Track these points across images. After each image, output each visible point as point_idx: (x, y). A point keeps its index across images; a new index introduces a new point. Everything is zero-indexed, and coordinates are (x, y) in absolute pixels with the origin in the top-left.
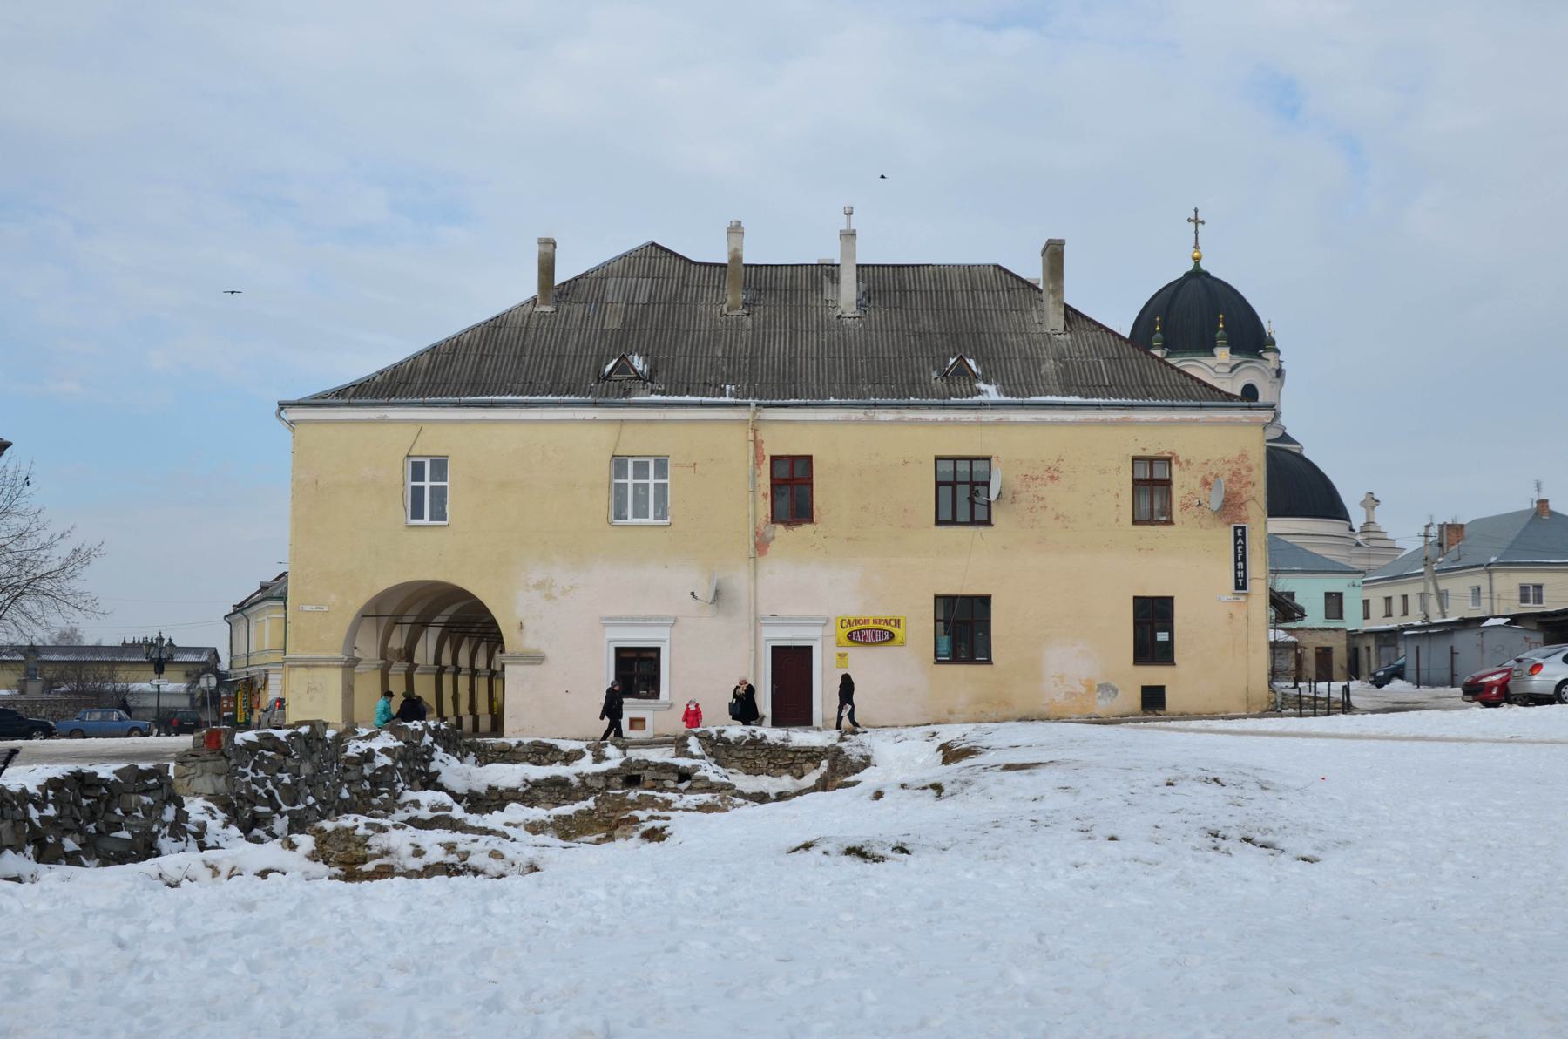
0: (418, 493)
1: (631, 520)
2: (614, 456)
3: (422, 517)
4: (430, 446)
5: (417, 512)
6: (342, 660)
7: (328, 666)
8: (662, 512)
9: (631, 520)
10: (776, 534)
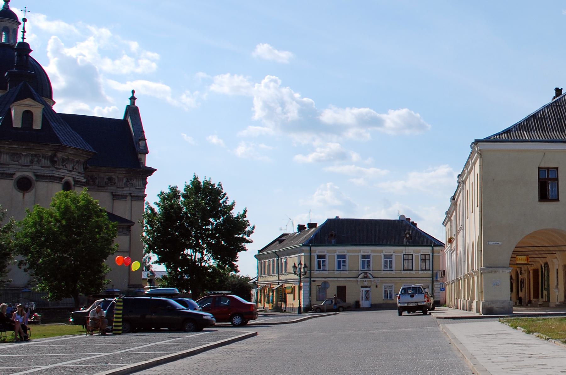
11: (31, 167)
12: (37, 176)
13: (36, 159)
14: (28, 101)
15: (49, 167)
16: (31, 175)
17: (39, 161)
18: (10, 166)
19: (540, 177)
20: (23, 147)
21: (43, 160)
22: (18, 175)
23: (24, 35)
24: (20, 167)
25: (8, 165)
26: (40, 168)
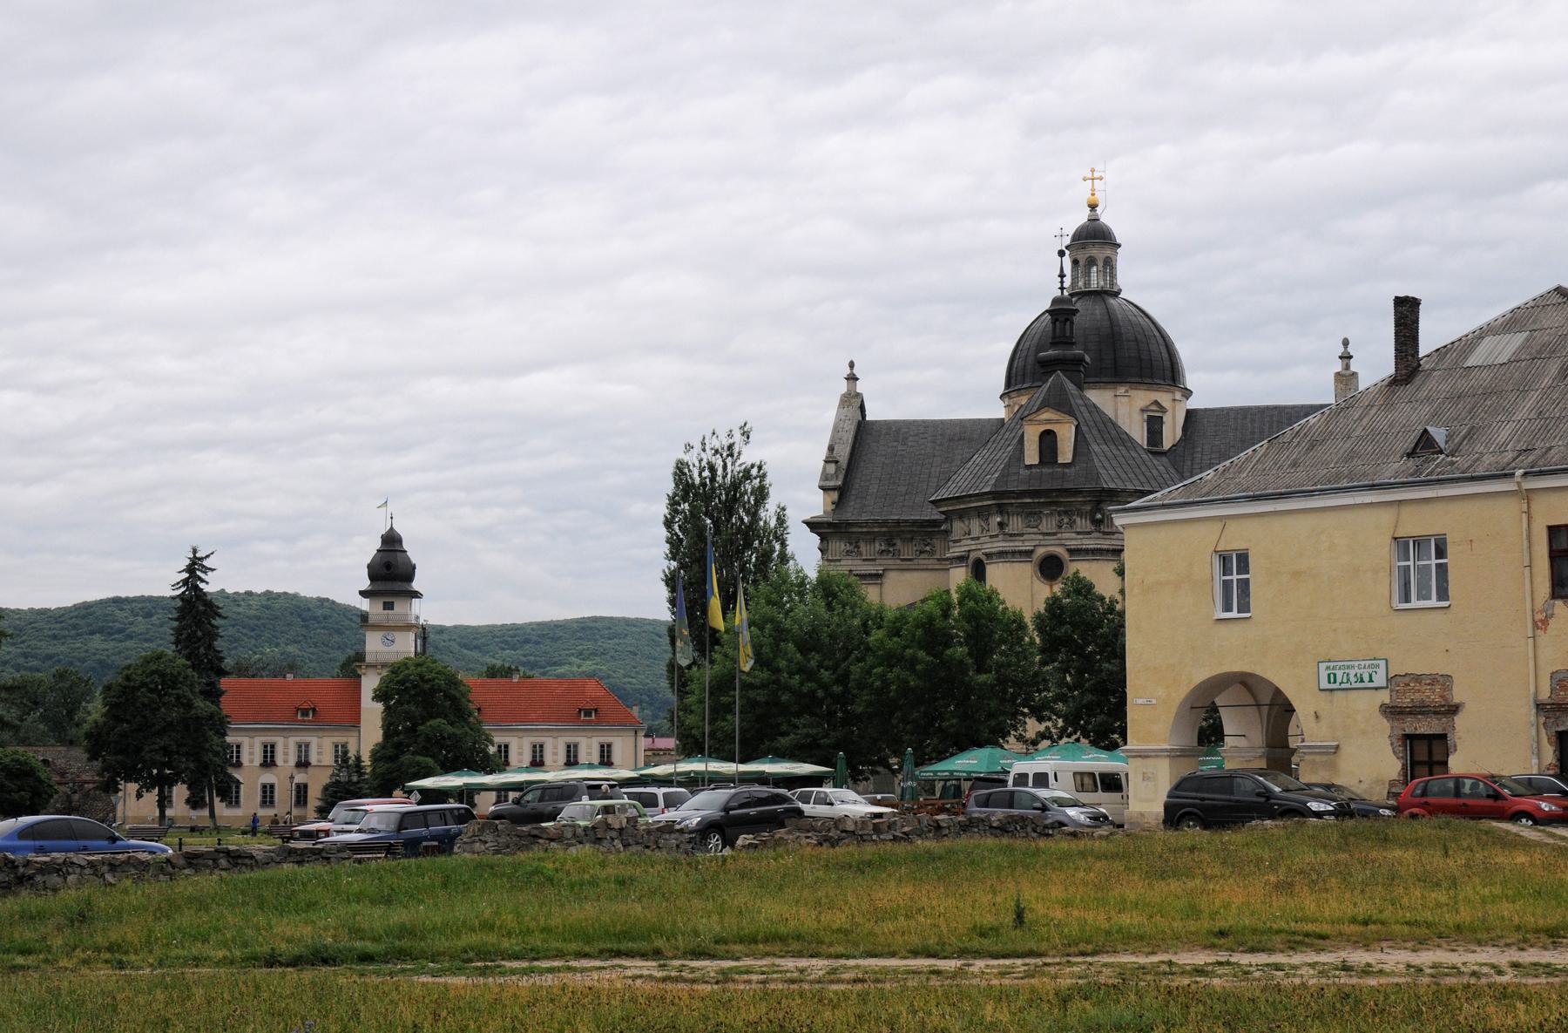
0: (1227, 585)
1: (1415, 603)
2: (1395, 539)
3: (1230, 610)
4: (1235, 540)
5: (1228, 608)
6: (1166, 750)
7: (1157, 756)
8: (1443, 594)
9: (1415, 603)
10: (1556, 611)
11: (1059, 535)
12: (1072, 552)
13: (1066, 520)
14: (1045, 415)
15: (1089, 533)
16: (1060, 551)
17: (1072, 524)
18: (1025, 537)
19: (1554, 547)
20: (1042, 500)
21: (1078, 520)
22: (1041, 551)
23: (1062, 282)
24: (1041, 537)
25: (1022, 535)
26: (1074, 535)
